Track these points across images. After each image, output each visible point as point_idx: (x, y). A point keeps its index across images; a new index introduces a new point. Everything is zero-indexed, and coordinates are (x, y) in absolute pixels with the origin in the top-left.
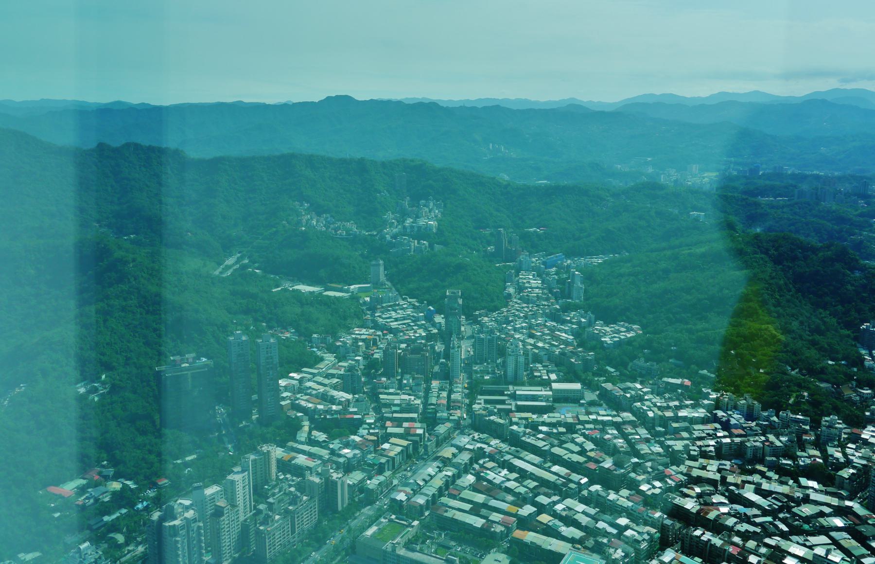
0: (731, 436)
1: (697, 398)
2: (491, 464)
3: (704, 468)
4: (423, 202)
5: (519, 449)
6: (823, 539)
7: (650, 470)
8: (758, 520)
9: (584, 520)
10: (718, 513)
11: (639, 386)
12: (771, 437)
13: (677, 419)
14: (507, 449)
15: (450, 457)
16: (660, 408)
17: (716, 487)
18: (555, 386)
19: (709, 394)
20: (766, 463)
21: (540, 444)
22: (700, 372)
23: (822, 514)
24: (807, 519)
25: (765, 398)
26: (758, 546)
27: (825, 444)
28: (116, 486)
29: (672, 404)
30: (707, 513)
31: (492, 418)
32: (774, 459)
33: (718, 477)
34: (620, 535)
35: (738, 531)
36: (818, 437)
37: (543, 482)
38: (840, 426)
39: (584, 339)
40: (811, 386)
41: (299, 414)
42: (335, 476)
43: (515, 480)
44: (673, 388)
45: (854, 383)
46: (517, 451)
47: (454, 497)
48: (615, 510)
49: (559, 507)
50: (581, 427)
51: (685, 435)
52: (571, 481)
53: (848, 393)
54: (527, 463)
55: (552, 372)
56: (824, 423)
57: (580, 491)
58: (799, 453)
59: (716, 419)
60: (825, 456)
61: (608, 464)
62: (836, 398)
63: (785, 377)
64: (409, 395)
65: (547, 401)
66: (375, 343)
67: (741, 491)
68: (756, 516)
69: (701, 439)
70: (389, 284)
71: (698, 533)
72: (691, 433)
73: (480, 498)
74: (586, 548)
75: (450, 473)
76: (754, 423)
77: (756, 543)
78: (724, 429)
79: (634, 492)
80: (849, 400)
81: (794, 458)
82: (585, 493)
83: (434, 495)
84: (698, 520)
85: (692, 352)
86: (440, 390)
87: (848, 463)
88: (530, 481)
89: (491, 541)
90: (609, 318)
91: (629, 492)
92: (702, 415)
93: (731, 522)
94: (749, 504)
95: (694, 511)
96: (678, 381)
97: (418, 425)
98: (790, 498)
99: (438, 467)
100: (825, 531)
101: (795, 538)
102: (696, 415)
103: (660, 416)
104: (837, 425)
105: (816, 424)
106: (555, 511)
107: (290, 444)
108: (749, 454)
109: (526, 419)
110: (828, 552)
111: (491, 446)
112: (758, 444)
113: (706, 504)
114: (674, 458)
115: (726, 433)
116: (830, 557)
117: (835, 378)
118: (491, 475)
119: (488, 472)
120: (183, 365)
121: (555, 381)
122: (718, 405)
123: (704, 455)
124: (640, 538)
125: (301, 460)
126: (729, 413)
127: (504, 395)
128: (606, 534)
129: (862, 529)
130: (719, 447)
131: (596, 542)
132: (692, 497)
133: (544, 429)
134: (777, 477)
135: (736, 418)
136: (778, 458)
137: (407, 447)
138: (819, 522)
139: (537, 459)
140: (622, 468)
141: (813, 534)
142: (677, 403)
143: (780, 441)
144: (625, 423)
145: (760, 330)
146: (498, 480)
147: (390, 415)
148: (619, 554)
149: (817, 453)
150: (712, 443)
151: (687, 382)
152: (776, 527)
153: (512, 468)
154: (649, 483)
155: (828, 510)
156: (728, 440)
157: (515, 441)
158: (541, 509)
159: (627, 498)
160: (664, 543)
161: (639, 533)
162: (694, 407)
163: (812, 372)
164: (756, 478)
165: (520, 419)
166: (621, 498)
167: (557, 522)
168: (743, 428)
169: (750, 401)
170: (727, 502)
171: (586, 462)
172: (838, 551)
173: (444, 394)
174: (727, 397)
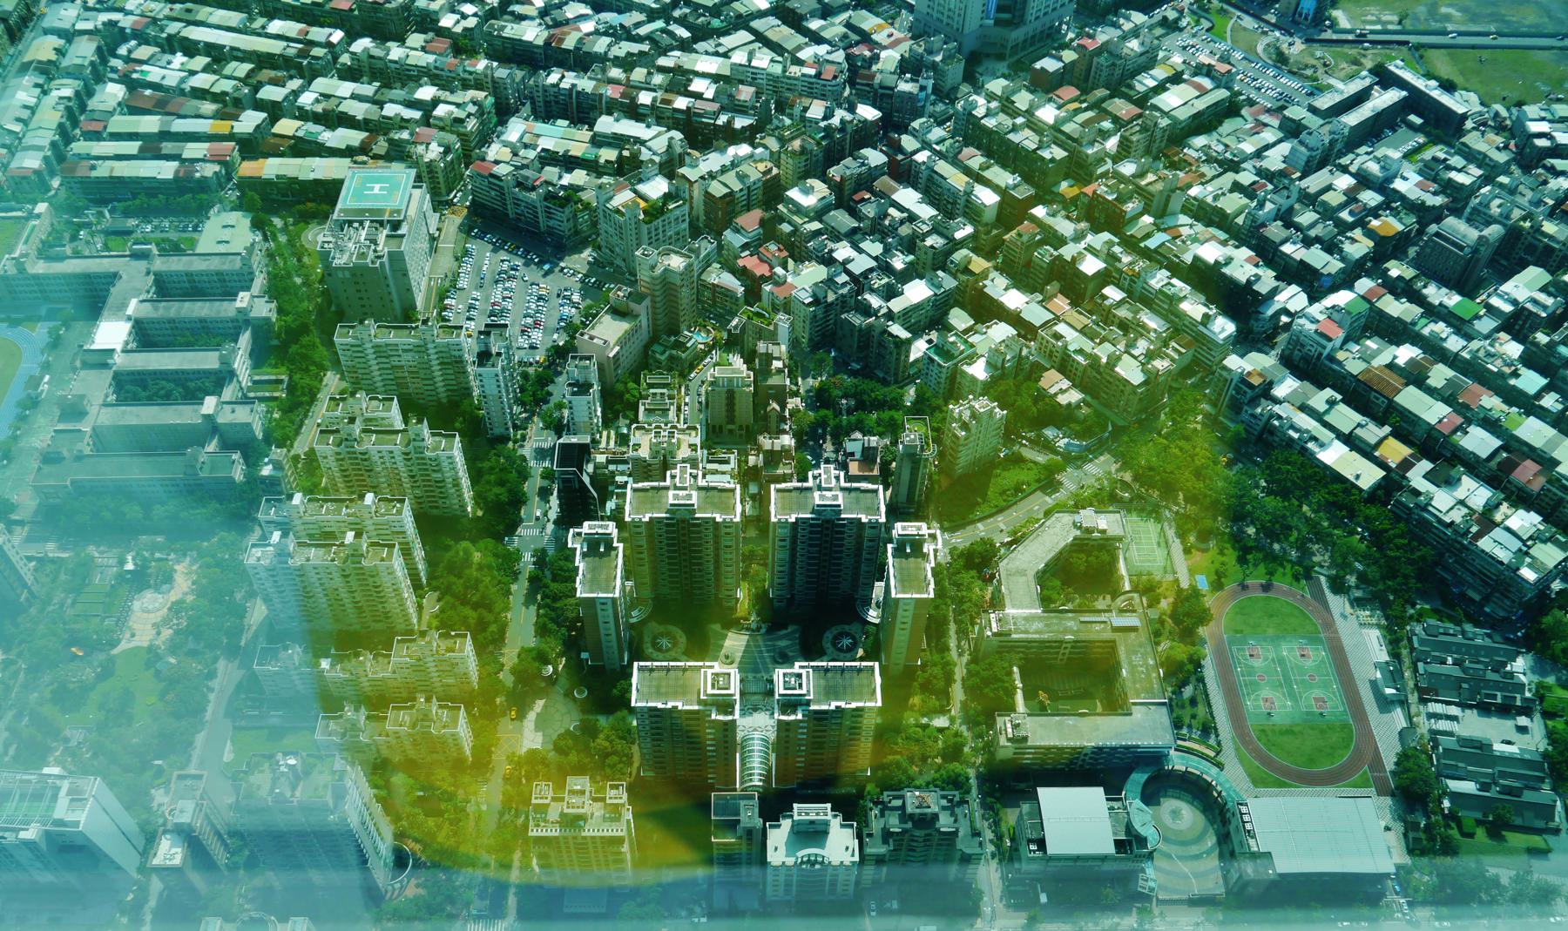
2: (144, 52)
5: (189, 5)
6: (743, 36)
8: (643, 31)
9: (359, 110)
10: (580, 35)
14: (166, 12)
15: (53, 57)
26: (649, 73)
30: (561, 40)
34: (427, 120)
35: (616, 58)
37: (263, 61)
43: (205, 70)
46: (189, 11)
47: (96, 136)
48: (407, 76)
49: (307, 99)
52: (313, 44)
57: (335, 58)
68: (638, 25)
71: (553, 78)
73: (150, 124)
74: (376, 157)
77: (645, 71)
79: (431, 35)
82: (345, 59)
83: (53, 144)
88: (234, 64)
89: (205, 196)
91: (423, 36)
93: (600, 46)
95: (540, 42)
101: (701, 46)
106: (301, 108)
110: (751, 55)
111: (130, 13)
118: (154, 74)
119: (145, 67)
124: (461, 114)
128: (404, 123)
131: (391, 142)
132: (532, 18)
138: (734, 10)
141: (726, 33)
146: (172, 79)
148: (434, 152)
152: (671, 34)
153: (190, 48)
154: (453, 12)
158: (275, 111)
159: (423, 49)
160: (504, 112)
161: (458, 105)
166: (411, 51)
170: (589, 11)
172: (765, 50)
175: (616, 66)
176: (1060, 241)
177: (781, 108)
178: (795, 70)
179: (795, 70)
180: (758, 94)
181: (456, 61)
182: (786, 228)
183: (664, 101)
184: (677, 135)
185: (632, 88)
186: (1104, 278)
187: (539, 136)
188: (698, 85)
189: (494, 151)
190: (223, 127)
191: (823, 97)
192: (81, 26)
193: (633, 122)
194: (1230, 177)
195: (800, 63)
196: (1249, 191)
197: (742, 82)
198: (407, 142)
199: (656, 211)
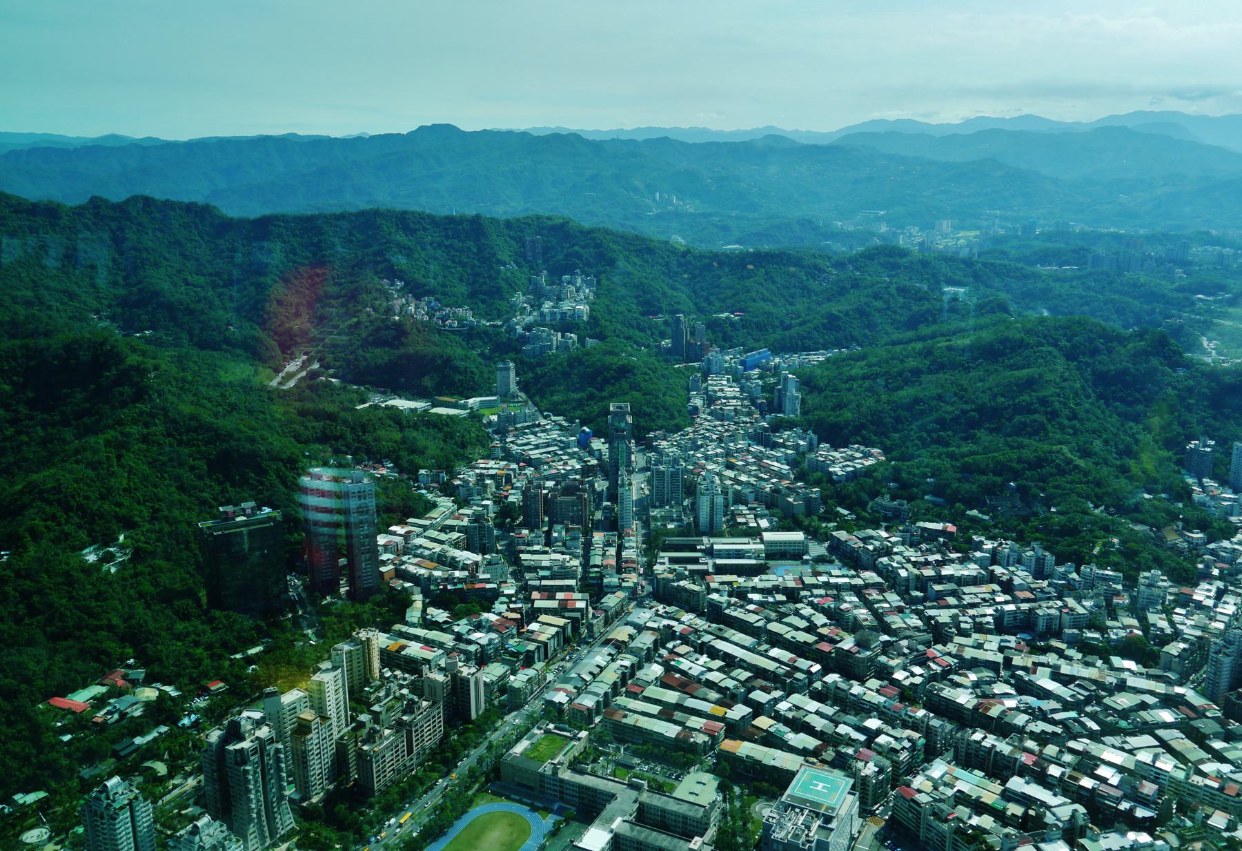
0: (1015, 600)
1: (966, 548)
2: (683, 649)
3: (979, 646)
4: (566, 277)
5: (721, 626)
7: (906, 651)
9: (819, 723)
11: (884, 534)
12: (1071, 602)
13: (940, 579)
14: (706, 627)
15: (626, 639)
16: (915, 564)
17: (997, 672)
18: (768, 536)
19: (982, 543)
20: (1065, 638)
21: (752, 618)
22: (968, 512)
23: (1143, 706)
24: (1124, 714)
25: (1059, 548)
26: (1061, 752)
27: (1145, 609)
28: (150, 694)
29: (931, 558)
30: (988, 709)
31: (682, 583)
32: (1076, 631)
33: (999, 658)
35: (1032, 732)
36: (1134, 599)
37: (759, 672)
38: (1165, 584)
39: (804, 470)
40: (1122, 529)
41: (407, 585)
42: (466, 671)
43: (719, 670)
44: (931, 536)
45: (1180, 524)
46: (720, 630)
47: (634, 696)
49: (783, 706)
50: (808, 593)
51: (952, 600)
52: (798, 669)
53: (1172, 538)
54: (735, 644)
55: (762, 516)
56: (1142, 581)
57: (811, 682)
58: (1109, 623)
59: (992, 578)
60: (1145, 626)
61: (848, 643)
62: (1157, 545)
63: (1086, 518)
64: (563, 553)
65: (758, 557)
66: (508, 480)
67: (1032, 677)
68: (1054, 711)
69: (973, 606)
70: (522, 395)
71: (978, 736)
72: (959, 599)
73: (672, 696)
74: (823, 761)
75: (627, 663)
76: (1045, 583)
78: (1004, 592)
79: (886, 683)
80: (1173, 548)
81: (1103, 630)
82: (818, 685)
83: (606, 694)
84: (977, 718)
85: (955, 485)
86: (605, 546)
87: (1177, 635)
88: (740, 670)
89: (691, 756)
90: (837, 437)
91: (879, 682)
92: (974, 573)
93: (1021, 719)
94: (1045, 694)
96: (938, 526)
97: (577, 595)
98: (1100, 685)
99: (610, 654)
100: (1148, 728)
102: (966, 573)
103: (917, 576)
104: (1160, 583)
105: (1131, 582)
106: (777, 712)
107: (397, 627)
108: (1041, 625)
109: (730, 583)
110: (1156, 757)
111: (683, 623)
112: (1053, 611)
113: (985, 696)
114: (939, 634)
115: (1008, 598)
116: (1158, 764)
117: (1153, 517)
118: (685, 664)
119: (681, 659)
120: (238, 519)
121: (771, 529)
122: (995, 558)
123: (979, 628)
124: (898, 747)
125: (415, 650)
126: (1012, 569)
127: (696, 550)
128: (850, 742)
129: (1199, 724)
130: (999, 618)
131: (838, 753)
132: (966, 687)
133: (756, 597)
134: (1079, 656)
135: (1021, 576)
136: (1081, 629)
137: (564, 628)
138: (1141, 717)
139: (748, 640)
140: (868, 649)
141: (1133, 734)
142: (938, 557)
143: (1083, 607)
144: (867, 586)
145: (1051, 452)
146: (695, 670)
147: (537, 583)
148: (870, 769)
149: (1135, 622)
150: (990, 611)
151: (951, 528)
152: (1083, 725)
153: (713, 653)
155: (1151, 700)
156: (1012, 607)
157: (715, 614)
158: (758, 709)
159: (878, 691)
160: (931, 753)
161: (896, 739)
162: (962, 561)
163: (1122, 510)
164: (1052, 658)
165: (722, 583)
166: (869, 691)
167: (781, 727)
168: (1032, 590)
169: (1040, 552)
171: (816, 642)
172: (1168, 756)
173: (612, 551)
174: (1007, 547)
175: (1031, 739)
177: (1183, 809)
178: (1197, 779)
179: (1197, 779)
180: (1160, 792)
181: (901, 706)
183: (1070, 777)
184: (1082, 810)
185: (1043, 761)
187: (957, 779)
188: (1103, 771)
189: (918, 782)
190: (719, 711)
191: (1225, 809)
192: (650, 624)
193: (1041, 788)
195: (1204, 775)
197: (1145, 778)
198: (851, 756)
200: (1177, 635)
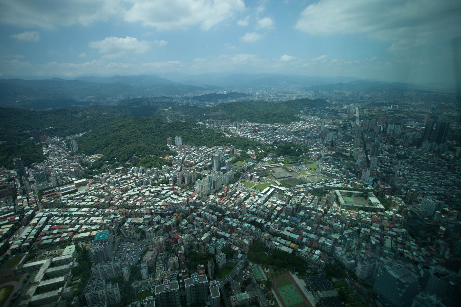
2: (56, 218)
3: (134, 191)
6: (170, 198)
9: (99, 221)
15: (36, 222)
16: (115, 178)
18: (76, 182)
21: (76, 204)
23: (167, 192)
24: (164, 195)
33: (138, 192)
37: (80, 216)
51: (125, 183)
59: (133, 176)
60: (165, 176)
61: (103, 200)
69: (130, 183)
71: (136, 210)
72: (127, 182)
114: (124, 191)
121: (75, 181)
123: (132, 188)
129: (177, 192)
139: (76, 209)
142: (121, 175)
155: (168, 190)
158: (82, 225)
167: (89, 226)
176: (229, 222)
179: (179, 202)
182: (181, 229)
184: (159, 216)
186: (237, 226)
194: (253, 206)
196: (256, 207)
199: (157, 230)
200: (170, 177)
